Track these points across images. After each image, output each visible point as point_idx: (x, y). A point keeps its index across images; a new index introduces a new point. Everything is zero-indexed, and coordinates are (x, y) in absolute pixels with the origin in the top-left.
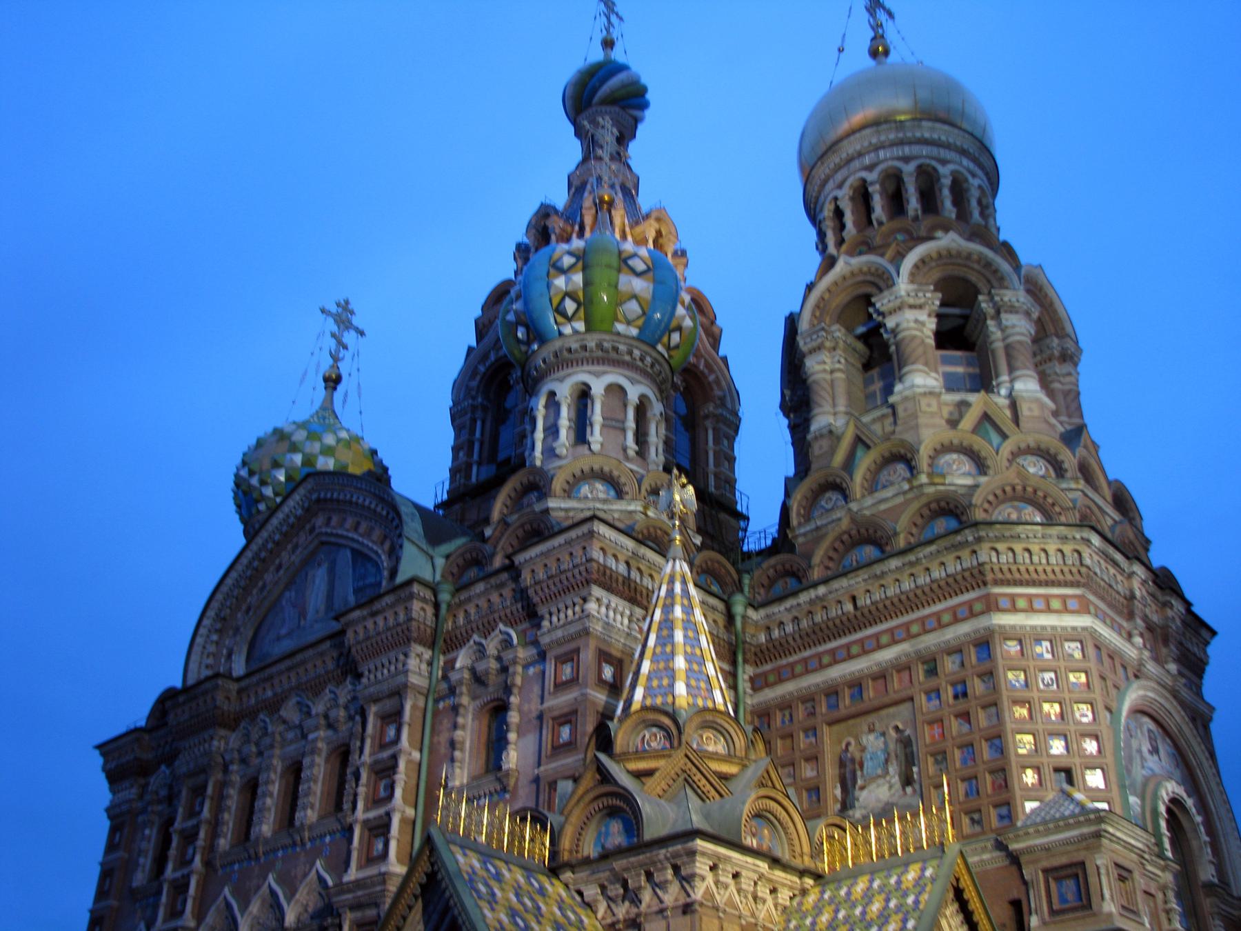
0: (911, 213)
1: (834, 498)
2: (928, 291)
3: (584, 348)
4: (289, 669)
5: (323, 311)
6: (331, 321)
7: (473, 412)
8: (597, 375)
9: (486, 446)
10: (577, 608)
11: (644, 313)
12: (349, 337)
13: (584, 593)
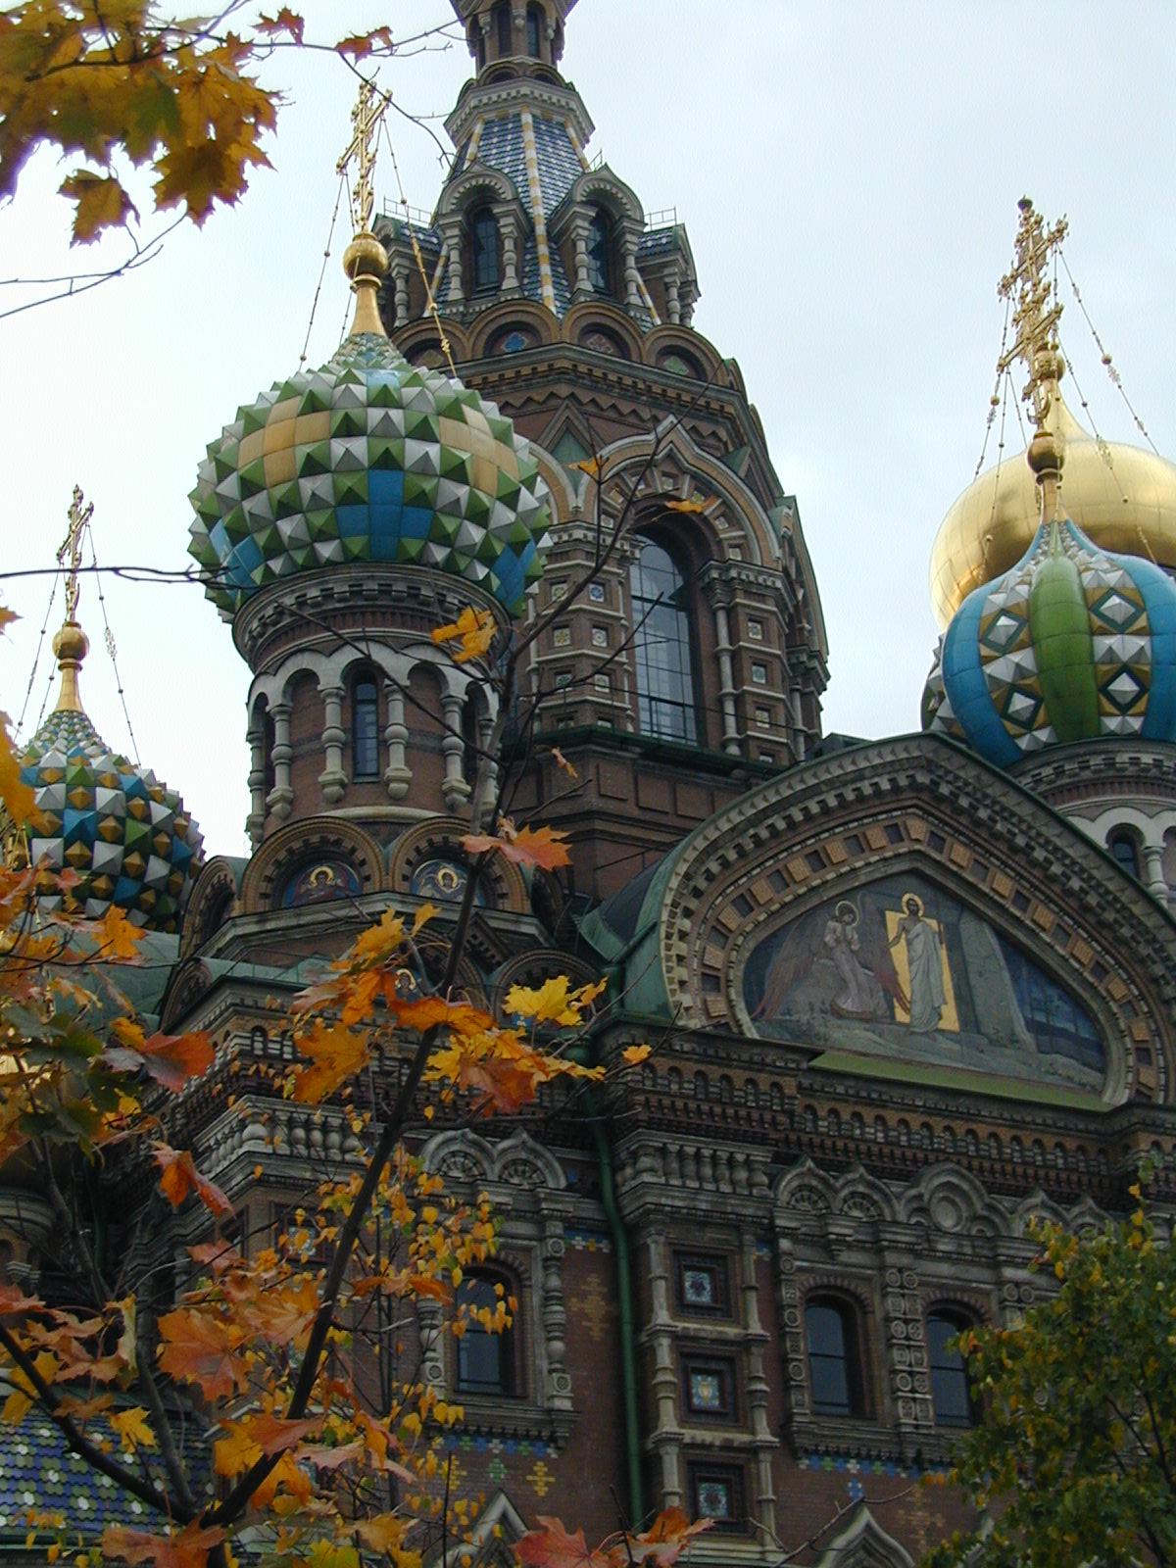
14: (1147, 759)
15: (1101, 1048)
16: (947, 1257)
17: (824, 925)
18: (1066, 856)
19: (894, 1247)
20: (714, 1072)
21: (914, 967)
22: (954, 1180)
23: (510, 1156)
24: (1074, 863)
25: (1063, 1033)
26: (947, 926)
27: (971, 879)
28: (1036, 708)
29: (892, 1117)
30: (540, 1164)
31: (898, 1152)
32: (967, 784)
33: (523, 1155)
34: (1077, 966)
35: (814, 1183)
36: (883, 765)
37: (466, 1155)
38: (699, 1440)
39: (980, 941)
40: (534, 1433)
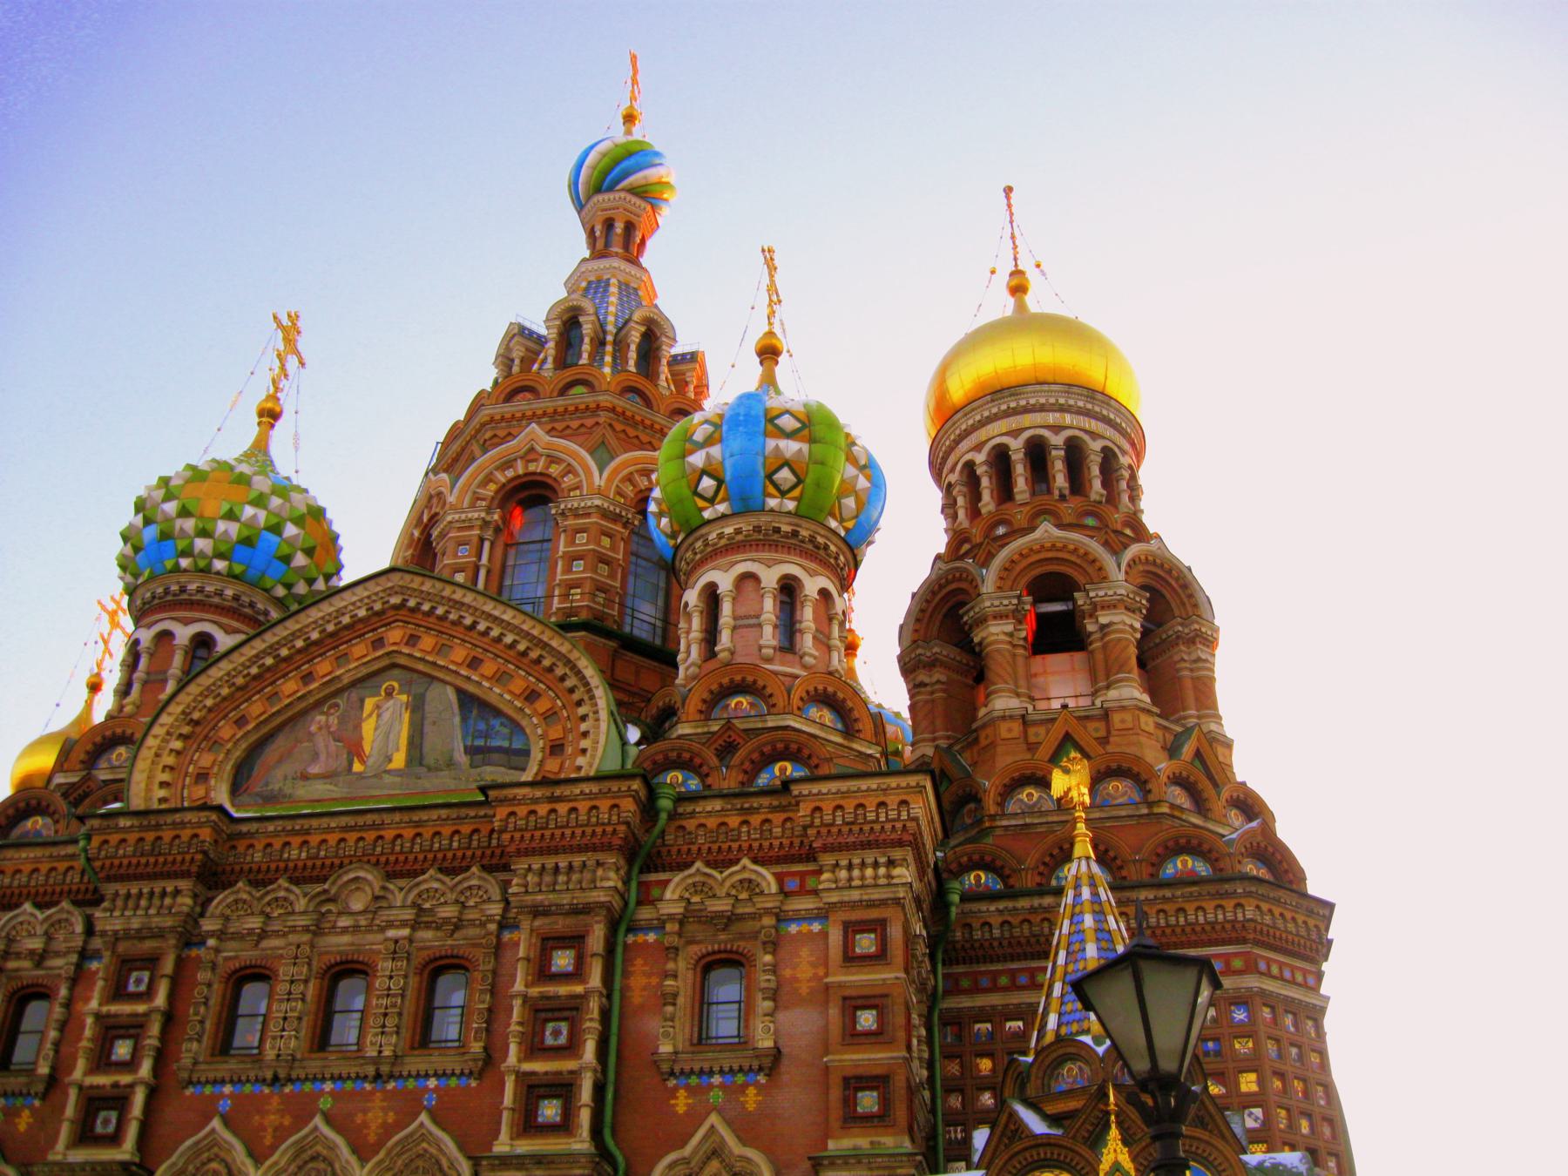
0: (1094, 497)
1: (1036, 796)
3: (795, 534)
5: (275, 317)
6: (280, 335)
7: (481, 528)
8: (812, 574)
10: (882, 871)
11: (857, 517)
12: (293, 362)
13: (897, 854)
14: (729, 530)
15: (526, 753)
16: (345, 930)
17: (313, 719)
18: (503, 621)
19: (293, 930)
20: (150, 836)
22: (361, 874)
23: (54, 918)
24: (509, 624)
25: (500, 749)
26: (415, 698)
28: (671, 521)
29: (314, 840)
30: (73, 919)
32: (429, 594)
33: (64, 916)
34: (507, 697)
36: (361, 600)
37: (29, 923)
39: (443, 699)
40: (25, 1091)
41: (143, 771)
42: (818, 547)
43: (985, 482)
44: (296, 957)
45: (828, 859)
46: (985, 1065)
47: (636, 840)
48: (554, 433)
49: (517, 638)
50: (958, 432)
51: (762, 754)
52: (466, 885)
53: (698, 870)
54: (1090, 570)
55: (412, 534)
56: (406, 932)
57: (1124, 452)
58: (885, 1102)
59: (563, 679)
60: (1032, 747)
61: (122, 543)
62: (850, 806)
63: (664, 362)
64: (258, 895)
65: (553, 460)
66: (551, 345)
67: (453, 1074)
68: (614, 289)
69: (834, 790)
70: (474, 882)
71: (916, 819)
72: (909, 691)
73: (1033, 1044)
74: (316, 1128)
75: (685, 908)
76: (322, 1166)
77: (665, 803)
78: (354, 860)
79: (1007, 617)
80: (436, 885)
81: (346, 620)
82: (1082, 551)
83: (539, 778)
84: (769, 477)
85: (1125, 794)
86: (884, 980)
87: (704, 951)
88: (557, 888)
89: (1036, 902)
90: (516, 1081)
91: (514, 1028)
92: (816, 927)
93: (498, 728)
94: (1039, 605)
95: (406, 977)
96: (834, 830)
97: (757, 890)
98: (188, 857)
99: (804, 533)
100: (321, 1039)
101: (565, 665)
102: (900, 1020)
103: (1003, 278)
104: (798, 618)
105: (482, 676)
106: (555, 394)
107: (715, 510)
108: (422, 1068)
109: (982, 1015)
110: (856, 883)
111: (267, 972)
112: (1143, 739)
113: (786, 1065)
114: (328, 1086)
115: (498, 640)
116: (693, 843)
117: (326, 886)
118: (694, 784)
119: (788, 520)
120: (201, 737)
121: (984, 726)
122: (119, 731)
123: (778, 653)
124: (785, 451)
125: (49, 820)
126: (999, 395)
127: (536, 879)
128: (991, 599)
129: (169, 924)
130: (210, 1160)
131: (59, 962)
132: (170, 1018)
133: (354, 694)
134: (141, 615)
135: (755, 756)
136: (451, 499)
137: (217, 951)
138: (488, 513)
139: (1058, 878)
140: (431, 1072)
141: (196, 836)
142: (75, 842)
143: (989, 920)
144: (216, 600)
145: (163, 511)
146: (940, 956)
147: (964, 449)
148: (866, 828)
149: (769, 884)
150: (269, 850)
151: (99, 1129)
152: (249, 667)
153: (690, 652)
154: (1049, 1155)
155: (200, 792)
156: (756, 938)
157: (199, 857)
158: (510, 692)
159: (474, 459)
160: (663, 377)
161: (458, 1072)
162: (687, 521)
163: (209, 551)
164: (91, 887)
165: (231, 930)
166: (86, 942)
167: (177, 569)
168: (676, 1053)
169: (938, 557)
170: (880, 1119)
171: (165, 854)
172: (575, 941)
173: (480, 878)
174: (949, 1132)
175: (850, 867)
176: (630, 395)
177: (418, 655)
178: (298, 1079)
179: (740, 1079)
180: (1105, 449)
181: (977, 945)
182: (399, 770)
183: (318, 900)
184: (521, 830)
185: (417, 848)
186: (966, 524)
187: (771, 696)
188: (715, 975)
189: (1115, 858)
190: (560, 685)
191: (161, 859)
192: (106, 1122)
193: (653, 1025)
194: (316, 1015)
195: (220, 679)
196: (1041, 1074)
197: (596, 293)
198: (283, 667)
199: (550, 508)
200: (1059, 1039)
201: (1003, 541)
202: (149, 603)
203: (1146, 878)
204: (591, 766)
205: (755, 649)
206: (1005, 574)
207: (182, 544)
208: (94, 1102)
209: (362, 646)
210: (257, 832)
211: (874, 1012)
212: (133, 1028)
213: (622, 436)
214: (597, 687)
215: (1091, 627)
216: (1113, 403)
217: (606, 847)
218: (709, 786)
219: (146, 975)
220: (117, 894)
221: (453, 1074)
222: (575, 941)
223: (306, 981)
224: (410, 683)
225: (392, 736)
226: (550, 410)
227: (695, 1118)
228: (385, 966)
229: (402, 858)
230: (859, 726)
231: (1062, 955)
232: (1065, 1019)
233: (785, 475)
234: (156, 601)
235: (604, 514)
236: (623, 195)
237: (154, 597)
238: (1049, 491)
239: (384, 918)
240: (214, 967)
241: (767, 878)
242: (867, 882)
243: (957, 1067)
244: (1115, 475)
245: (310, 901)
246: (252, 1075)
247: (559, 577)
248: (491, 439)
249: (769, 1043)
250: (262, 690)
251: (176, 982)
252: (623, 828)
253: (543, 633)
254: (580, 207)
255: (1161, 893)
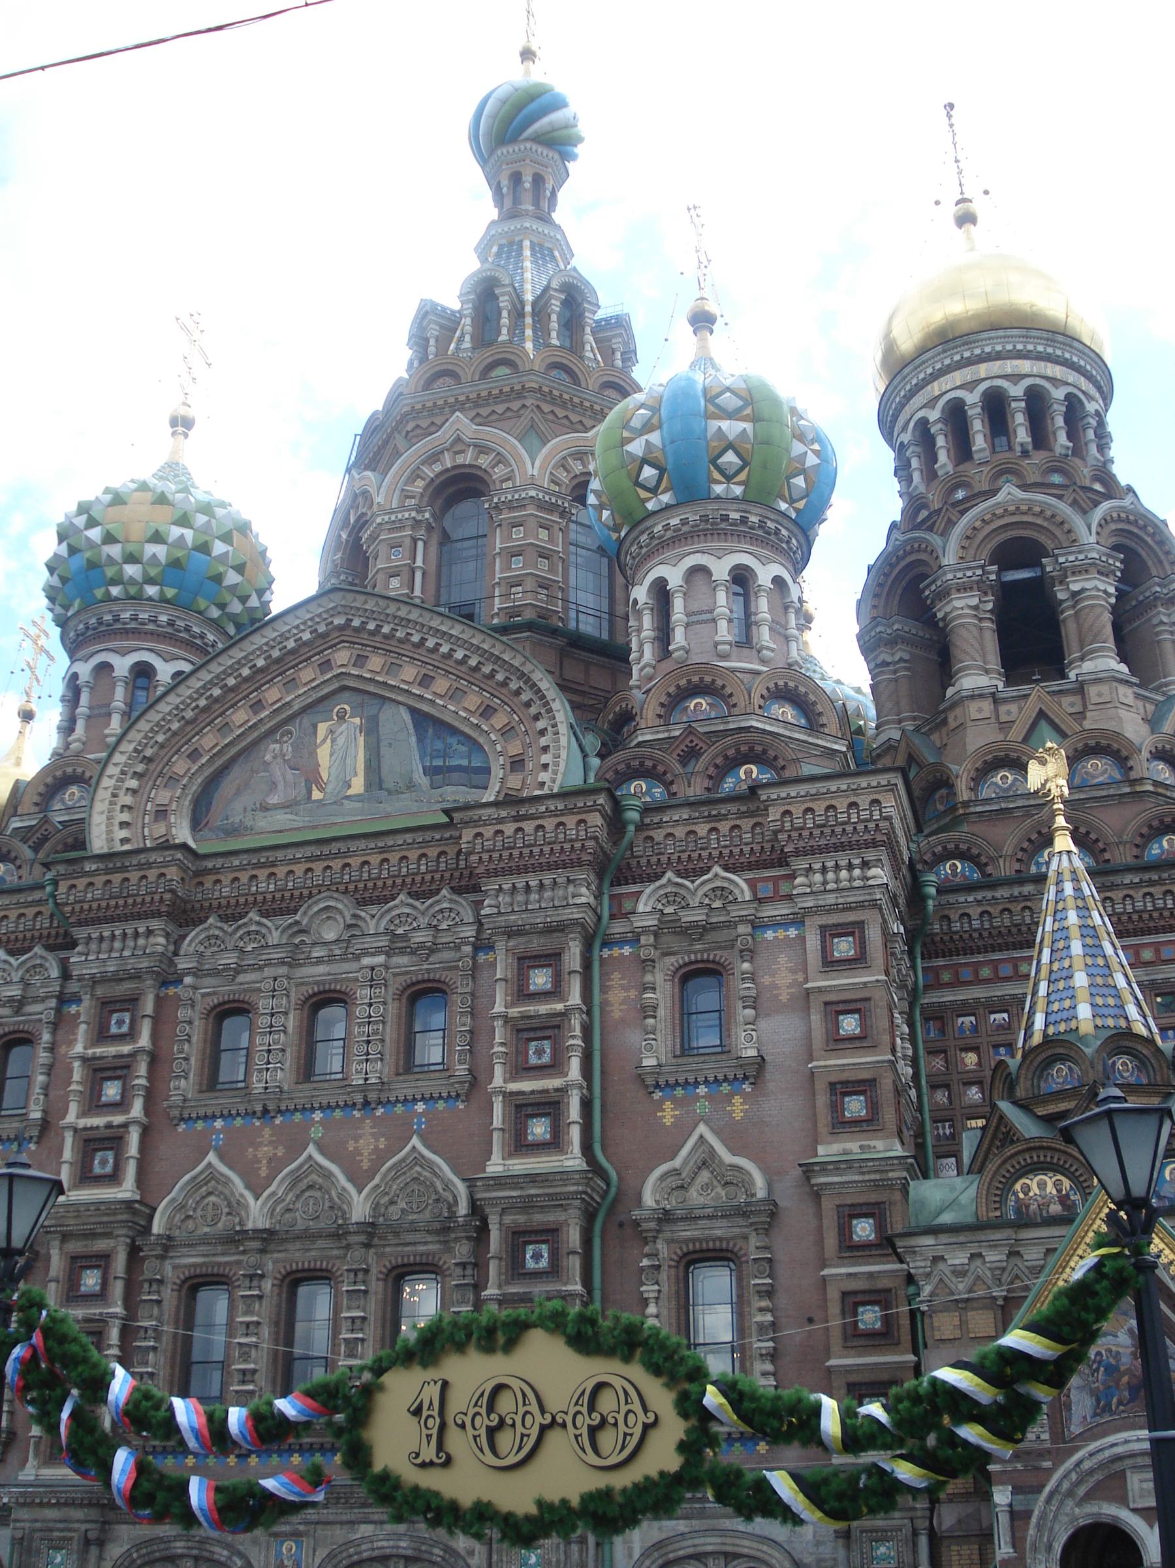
0: (1058, 450)
2: (1116, 559)
3: (744, 520)
4: (311, 859)
7: (413, 528)
9: (432, 579)
10: (857, 872)
11: (807, 496)
13: (871, 855)
14: (675, 521)
15: (487, 771)
16: (319, 961)
17: (266, 750)
18: (452, 636)
19: (269, 963)
20: (117, 878)
21: (334, 758)
23: (29, 965)
27: (381, 679)
28: (612, 514)
29: (281, 871)
30: (47, 965)
31: (287, 894)
33: (38, 962)
35: (217, 932)
36: (304, 623)
38: (89, 1125)
39: (395, 721)
41: (102, 813)
42: (769, 534)
43: (940, 441)
44: (275, 990)
45: (800, 864)
46: (971, 1059)
47: (605, 853)
48: (478, 420)
49: (467, 653)
50: (908, 387)
51: (726, 757)
52: (437, 908)
53: (669, 880)
54: (1058, 532)
55: (340, 536)
56: (381, 959)
57: (1090, 398)
58: (873, 1107)
59: (518, 693)
60: (1004, 726)
61: (46, 573)
62: (819, 807)
63: (588, 330)
64: (230, 930)
65: (482, 449)
66: (468, 321)
67: (440, 1097)
68: (527, 253)
69: (803, 793)
70: (445, 905)
71: (889, 819)
72: (870, 672)
73: (1020, 1044)
74: (310, 1157)
75: (659, 920)
76: (318, 1194)
77: (633, 815)
78: (323, 889)
79: (971, 588)
80: (407, 910)
81: (291, 644)
82: (1049, 513)
83: (501, 798)
84: (713, 461)
85: (1105, 772)
86: (865, 984)
87: (681, 962)
88: (530, 907)
89: (1016, 891)
90: (504, 1102)
91: (497, 1049)
92: (792, 932)
93: (455, 746)
94: (1004, 573)
95: (385, 1003)
96: (805, 833)
97: (731, 898)
98: (157, 897)
99: (754, 519)
100: (307, 1070)
101: (519, 678)
102: (884, 1023)
103: (949, 211)
104: (753, 610)
105: (435, 693)
106: (477, 378)
107: (660, 501)
108: (409, 1093)
109: (965, 1008)
110: (830, 886)
111: (246, 1006)
112: (1122, 713)
113: (770, 1073)
114: (318, 1116)
115: (449, 656)
116: (663, 854)
117: (297, 918)
118: (658, 792)
119: (735, 506)
120: (156, 774)
121: (953, 706)
122: (69, 770)
123: (735, 649)
124: (728, 433)
125: (11, 866)
126: (951, 344)
127: (508, 899)
128: (955, 571)
129: (145, 965)
130: (210, 1194)
131: (37, 1008)
132: (154, 1059)
133: (306, 720)
134: (74, 646)
135: (719, 761)
136: (379, 499)
137: (195, 988)
138: (418, 512)
139: (1038, 864)
140: (418, 1097)
141: (163, 875)
142: (42, 887)
143: (967, 911)
144: (151, 627)
145: (87, 538)
146: (918, 950)
147: (916, 406)
148: (838, 829)
149: (742, 891)
150: (236, 884)
151: (97, 1170)
152: (197, 699)
153: (643, 653)
154: (1042, 1159)
155: (160, 829)
156: (732, 947)
157: (167, 896)
158: (466, 709)
159: (397, 454)
160: (588, 347)
161: (445, 1095)
162: (630, 514)
163: (139, 578)
164: (62, 931)
165: (207, 967)
166: (62, 986)
167: (108, 598)
168: (659, 1065)
169: (894, 526)
170: (869, 1124)
171: (133, 895)
172: (551, 959)
173: (451, 901)
174: (937, 1128)
175: (824, 870)
176: (554, 373)
177: (368, 676)
178: (288, 1110)
179: (725, 1088)
180: (1069, 397)
181: (956, 937)
182: (359, 795)
183: (290, 932)
184: (488, 851)
185: (385, 874)
186: (922, 489)
187: (731, 695)
188: (691, 984)
189: (1097, 840)
190: (516, 700)
191: (130, 901)
192: (104, 1163)
193: (634, 1037)
194: (300, 1045)
195: (170, 713)
196: (1030, 1076)
197: (508, 258)
198: (231, 696)
199: (483, 502)
200: (1048, 1041)
201: (963, 507)
202: (83, 634)
203: (1130, 860)
204: (554, 782)
205: (711, 644)
206: (966, 543)
207: (110, 572)
208: (91, 1143)
209: (310, 669)
210: (223, 867)
211: (857, 1016)
212: (120, 1069)
213: (550, 417)
214: (554, 700)
215: (1061, 596)
216: (1076, 344)
217: (578, 864)
218: (675, 794)
219: (127, 1017)
220: (90, 938)
221: (440, 1097)
222: (551, 959)
223: (286, 1013)
224: (362, 705)
225: (348, 761)
226: (473, 396)
227: (684, 1129)
228: (363, 994)
229: (370, 884)
230: (823, 720)
231: (1046, 952)
232: (1052, 1018)
233: (730, 457)
234: (89, 633)
235: (541, 505)
236: (528, 145)
237: (87, 628)
238: (1011, 448)
239: (359, 946)
240: (193, 1006)
241: (741, 885)
242: (842, 885)
243: (942, 1063)
244: (1080, 424)
245: (283, 932)
246: (242, 1112)
247: (498, 576)
248: (413, 430)
249: (752, 1052)
250: (212, 721)
251: (157, 1020)
252: (591, 843)
253: (493, 646)
254: (483, 159)
255: (1146, 877)
